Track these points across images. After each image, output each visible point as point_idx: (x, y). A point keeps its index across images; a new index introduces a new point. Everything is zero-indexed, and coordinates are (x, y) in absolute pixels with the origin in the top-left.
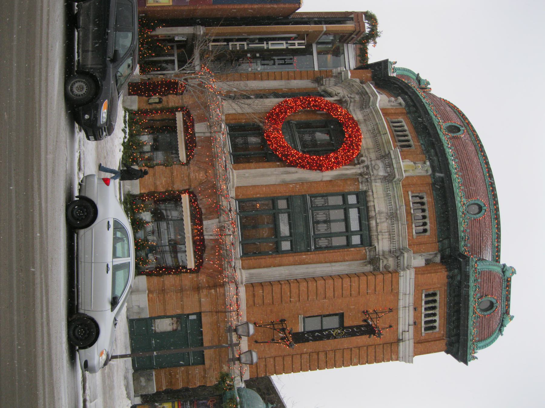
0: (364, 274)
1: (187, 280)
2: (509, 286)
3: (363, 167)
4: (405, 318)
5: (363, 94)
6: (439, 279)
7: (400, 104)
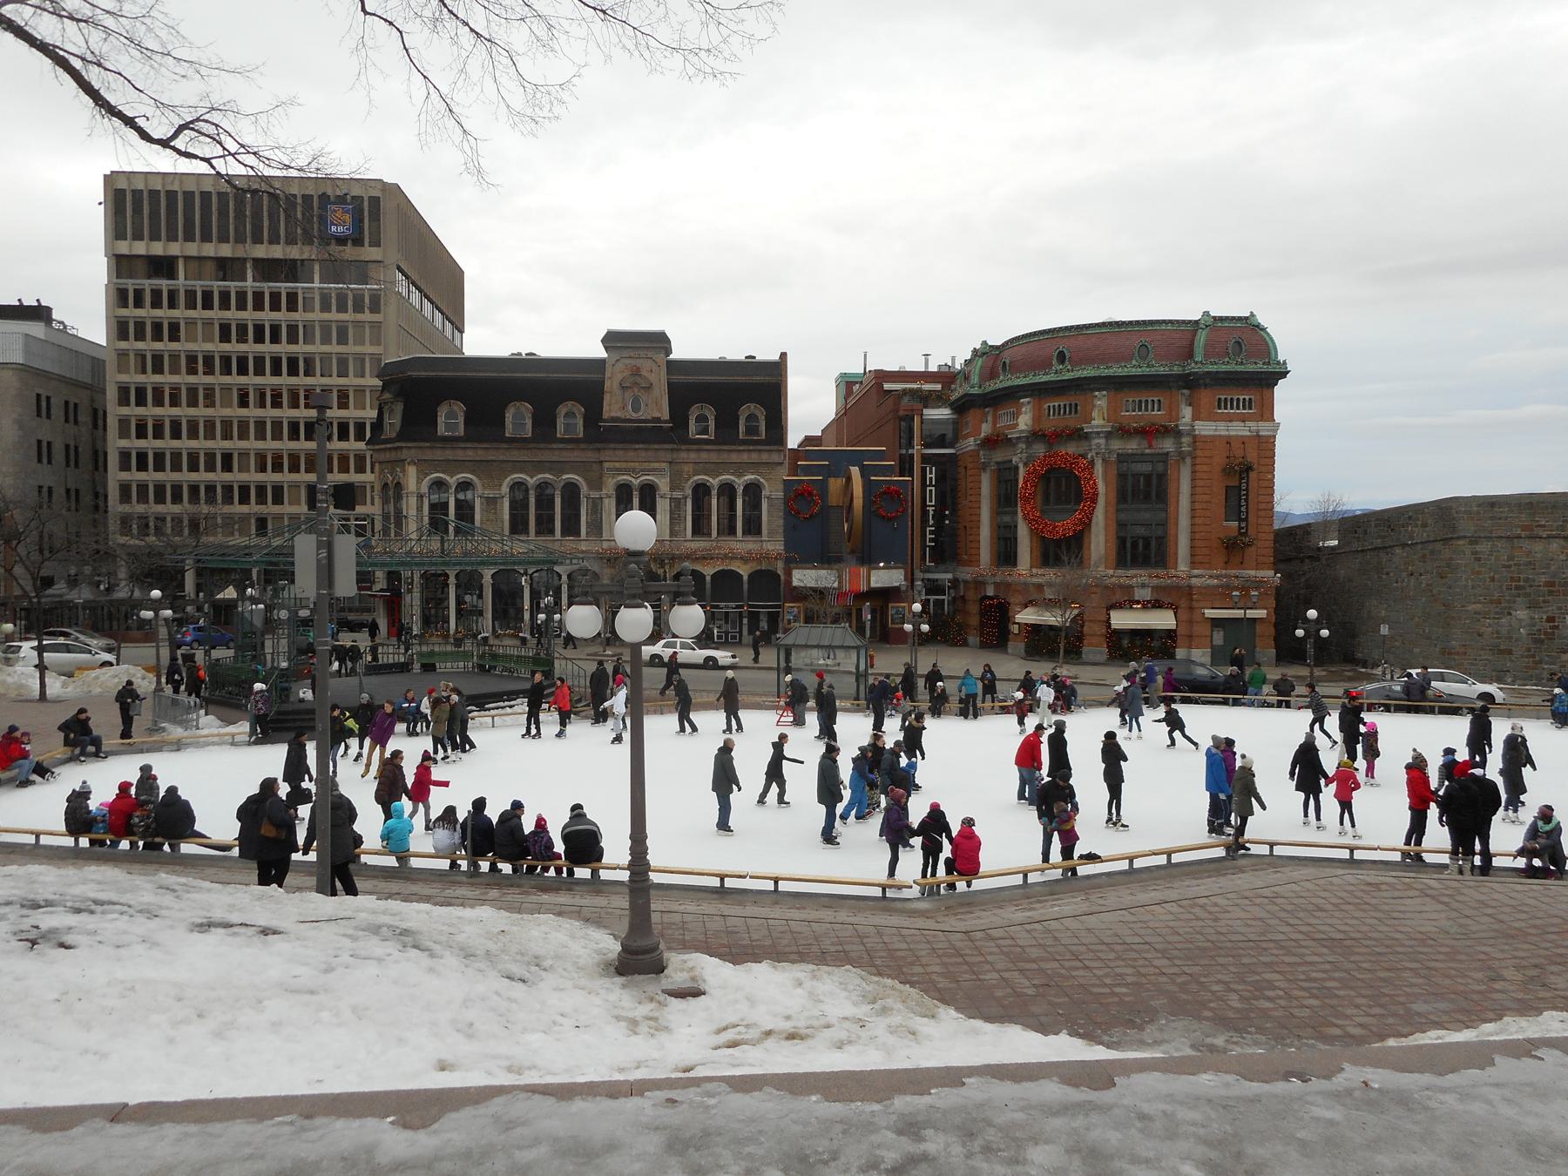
0: (1194, 465)
2: (1221, 319)
4: (1238, 429)
6: (1206, 397)
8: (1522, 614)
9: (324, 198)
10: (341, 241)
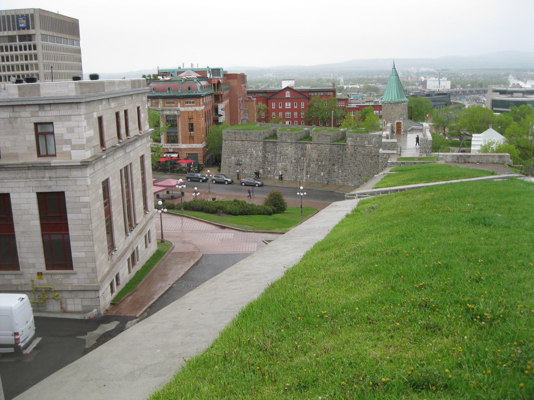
1: (180, 156)
8: (233, 158)
9: (18, 16)
10: (23, 28)
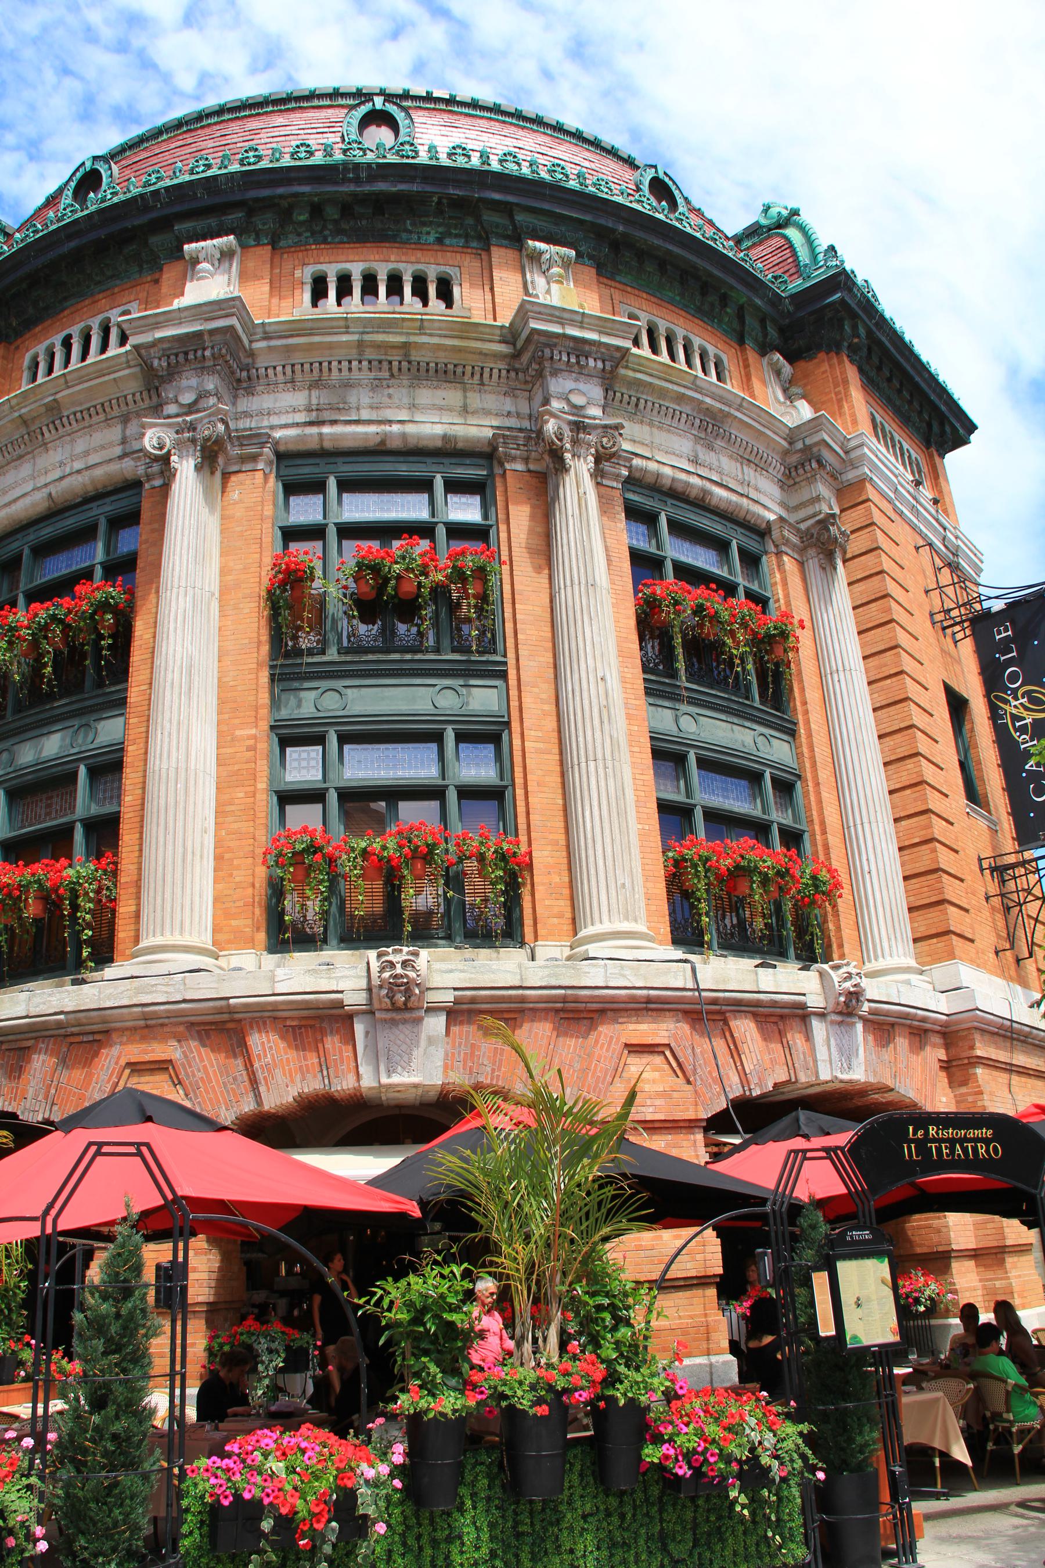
3: (575, 442)
5: (189, 351)
7: (226, 255)
